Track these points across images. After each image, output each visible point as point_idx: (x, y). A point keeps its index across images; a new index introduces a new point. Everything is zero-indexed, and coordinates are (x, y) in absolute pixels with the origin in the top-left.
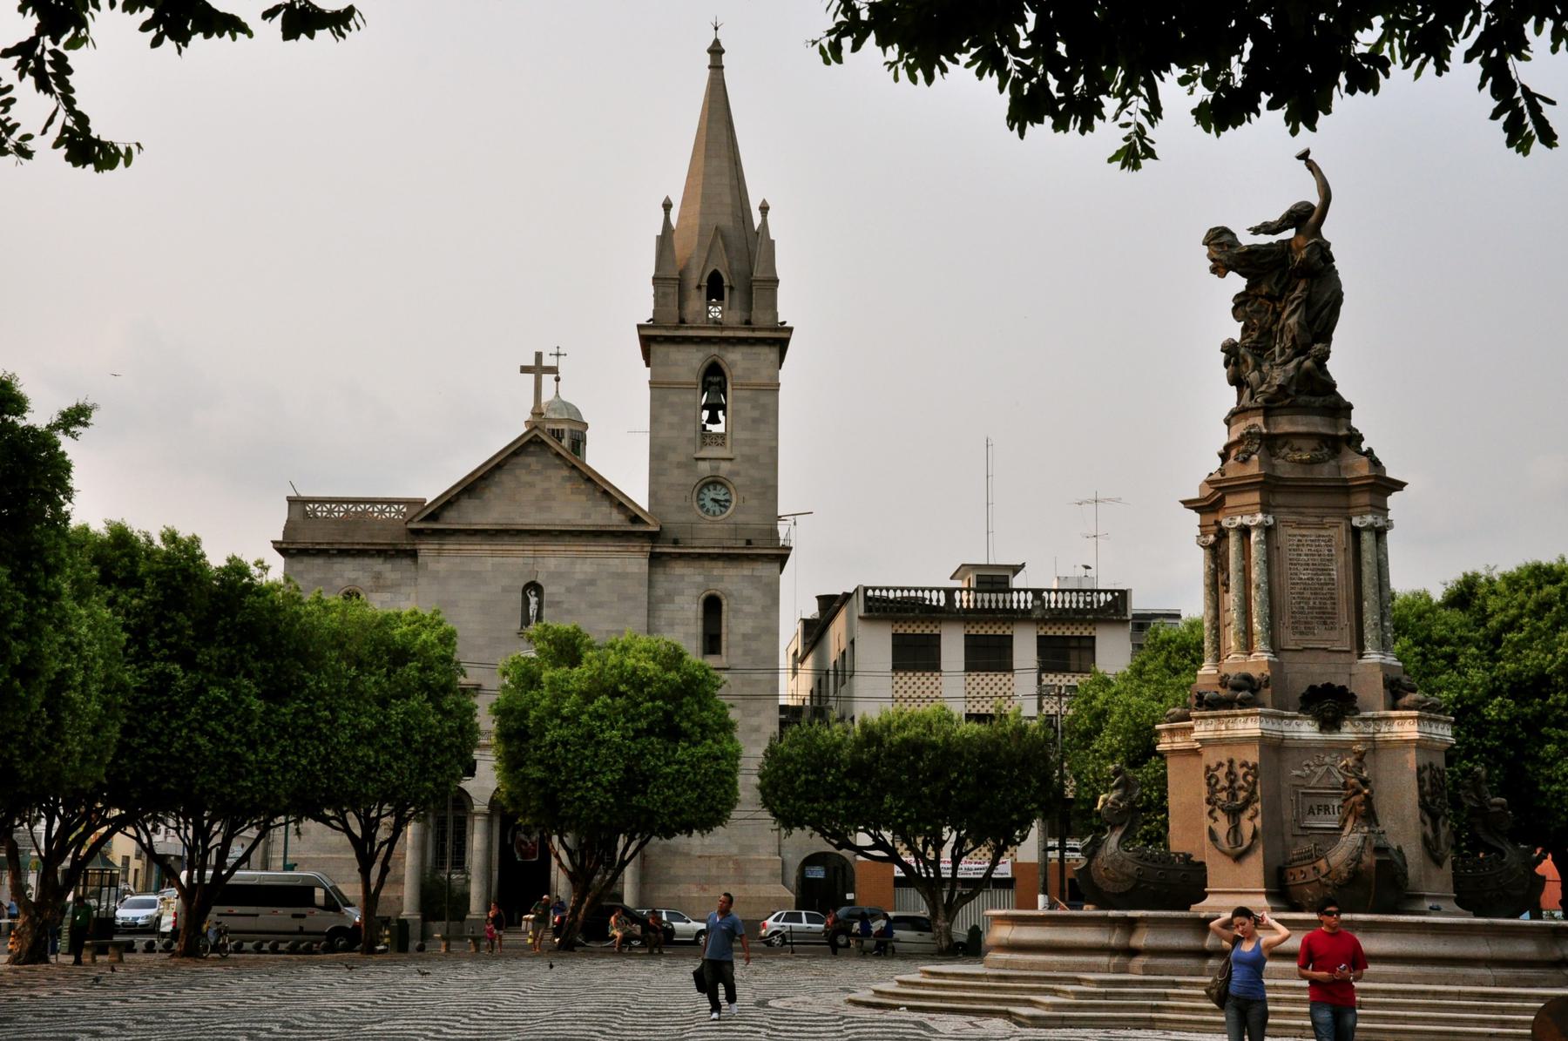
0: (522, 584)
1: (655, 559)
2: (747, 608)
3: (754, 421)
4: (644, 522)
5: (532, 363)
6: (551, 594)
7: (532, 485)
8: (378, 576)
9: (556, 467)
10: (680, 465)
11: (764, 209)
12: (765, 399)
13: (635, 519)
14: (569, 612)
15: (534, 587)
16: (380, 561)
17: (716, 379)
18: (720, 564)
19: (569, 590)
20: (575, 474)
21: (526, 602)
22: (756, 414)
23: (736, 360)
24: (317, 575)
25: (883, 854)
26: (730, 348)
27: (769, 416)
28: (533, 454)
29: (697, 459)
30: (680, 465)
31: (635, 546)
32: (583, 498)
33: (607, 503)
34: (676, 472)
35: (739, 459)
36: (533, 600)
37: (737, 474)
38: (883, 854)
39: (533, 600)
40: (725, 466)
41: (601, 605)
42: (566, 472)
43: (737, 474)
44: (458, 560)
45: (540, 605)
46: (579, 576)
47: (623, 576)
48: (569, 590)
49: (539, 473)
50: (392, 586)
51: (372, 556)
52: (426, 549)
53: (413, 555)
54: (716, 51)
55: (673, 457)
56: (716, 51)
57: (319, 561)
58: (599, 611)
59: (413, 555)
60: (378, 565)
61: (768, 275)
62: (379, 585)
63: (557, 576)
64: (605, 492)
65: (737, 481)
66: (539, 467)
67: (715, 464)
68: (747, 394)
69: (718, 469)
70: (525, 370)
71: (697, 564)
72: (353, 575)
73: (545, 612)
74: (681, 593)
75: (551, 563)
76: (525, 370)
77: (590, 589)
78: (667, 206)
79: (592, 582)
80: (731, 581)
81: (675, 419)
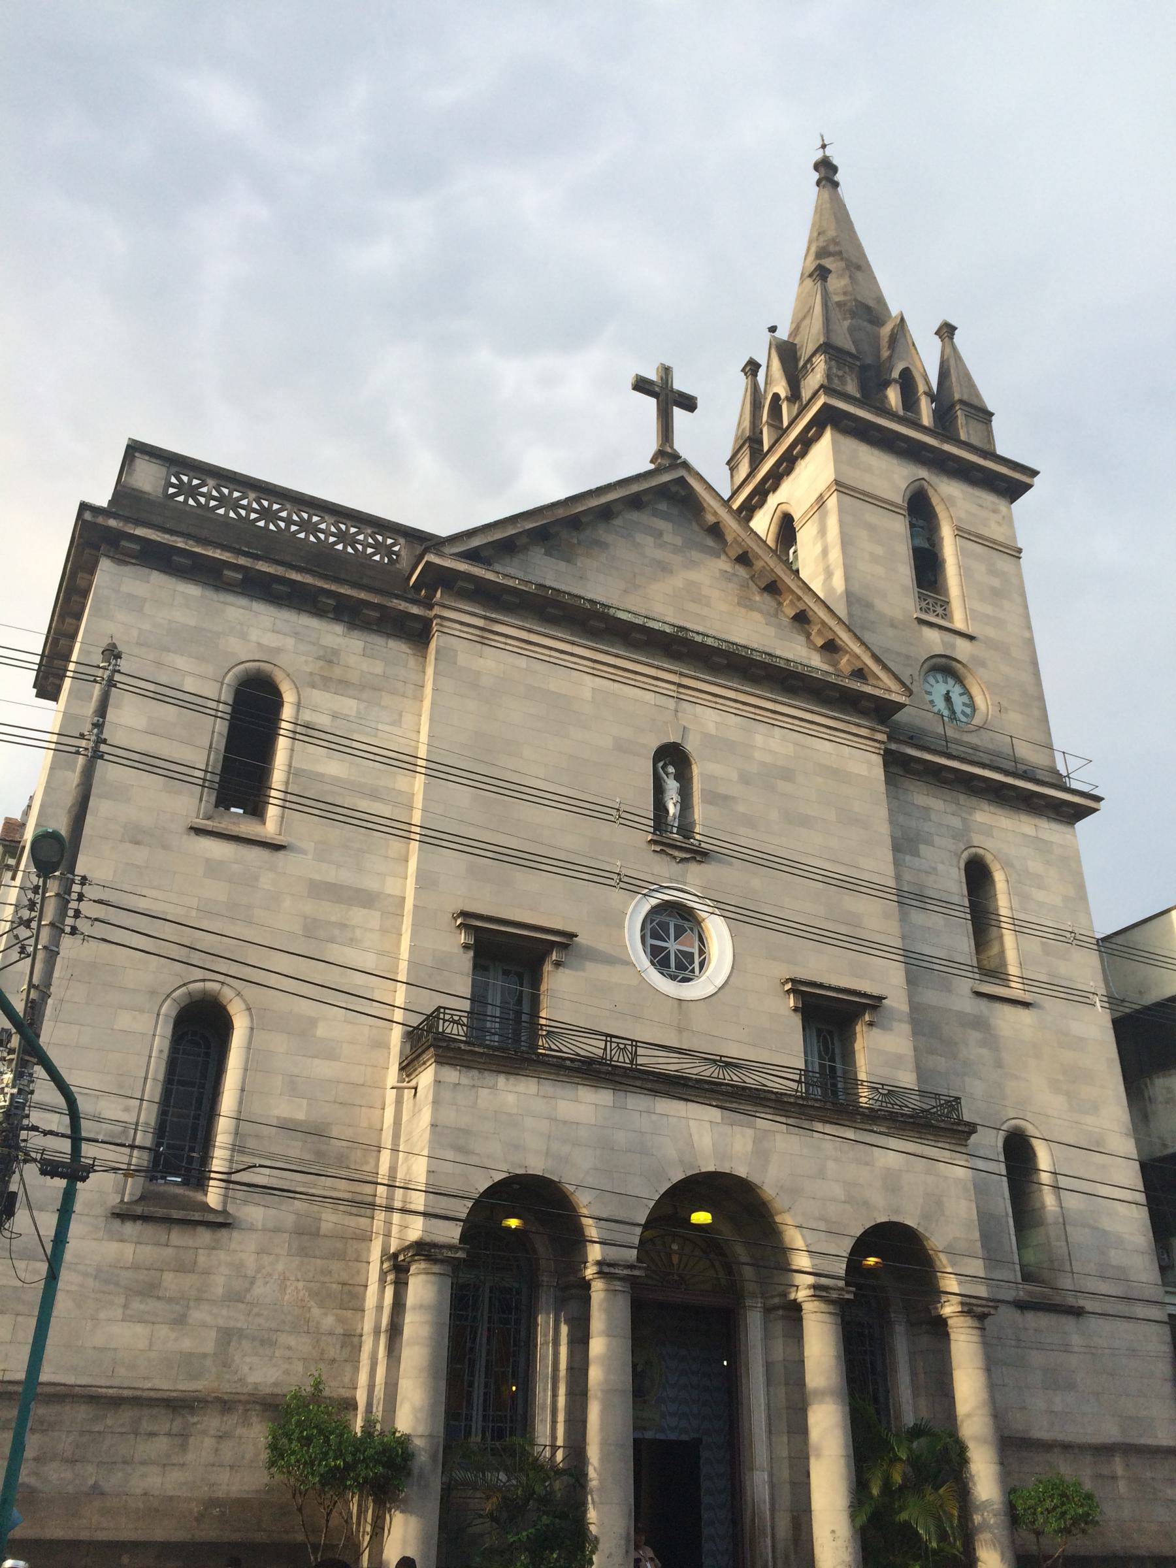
0: (654, 744)
7: (665, 569)
8: (330, 658)
11: (947, 331)
12: (1004, 564)
15: (672, 758)
16: (339, 628)
19: (745, 779)
22: (996, 582)
24: (184, 617)
26: (945, 479)
27: (1011, 592)
28: (666, 517)
29: (921, 621)
32: (756, 616)
36: (672, 786)
39: (672, 786)
40: (960, 643)
41: (805, 821)
44: (522, 662)
47: (838, 775)
48: (745, 779)
49: (677, 550)
50: (363, 687)
51: (319, 612)
54: (826, 170)
56: (826, 170)
57: (193, 591)
59: (417, 634)
62: (329, 677)
63: (719, 745)
66: (678, 541)
68: (979, 549)
70: (642, 385)
72: (271, 640)
77: (784, 786)
79: (787, 775)
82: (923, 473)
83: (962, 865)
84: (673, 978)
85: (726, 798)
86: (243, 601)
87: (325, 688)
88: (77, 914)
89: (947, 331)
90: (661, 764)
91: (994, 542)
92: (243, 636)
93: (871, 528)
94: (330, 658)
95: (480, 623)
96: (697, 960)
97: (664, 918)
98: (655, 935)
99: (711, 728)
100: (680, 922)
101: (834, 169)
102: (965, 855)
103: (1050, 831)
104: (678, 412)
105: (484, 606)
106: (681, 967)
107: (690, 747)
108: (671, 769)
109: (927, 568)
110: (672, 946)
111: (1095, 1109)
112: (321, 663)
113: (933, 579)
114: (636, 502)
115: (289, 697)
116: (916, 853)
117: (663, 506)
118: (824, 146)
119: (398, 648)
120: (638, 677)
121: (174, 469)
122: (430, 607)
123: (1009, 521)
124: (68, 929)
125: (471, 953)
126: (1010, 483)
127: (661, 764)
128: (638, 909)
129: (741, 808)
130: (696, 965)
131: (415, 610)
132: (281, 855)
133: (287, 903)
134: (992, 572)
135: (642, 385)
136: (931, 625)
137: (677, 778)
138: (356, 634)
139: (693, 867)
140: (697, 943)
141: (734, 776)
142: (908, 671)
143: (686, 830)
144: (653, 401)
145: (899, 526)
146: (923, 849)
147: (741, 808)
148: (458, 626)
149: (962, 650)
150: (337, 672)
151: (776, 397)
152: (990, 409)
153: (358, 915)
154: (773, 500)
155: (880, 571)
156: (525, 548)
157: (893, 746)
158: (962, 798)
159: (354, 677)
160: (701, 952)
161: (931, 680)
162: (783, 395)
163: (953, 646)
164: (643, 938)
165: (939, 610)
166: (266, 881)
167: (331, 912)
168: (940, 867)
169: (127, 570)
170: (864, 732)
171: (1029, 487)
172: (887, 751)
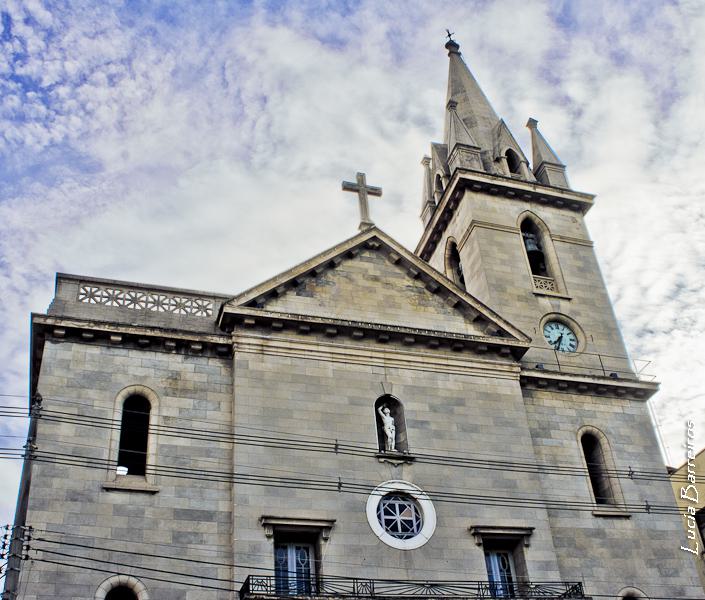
0: (376, 397)
1: (525, 382)
5: (354, 181)
11: (532, 123)
13: (501, 333)
15: (387, 402)
16: (179, 358)
21: (380, 423)
22: (580, 264)
23: (545, 214)
27: (589, 267)
30: (520, 298)
31: (504, 364)
34: (518, 304)
35: (575, 300)
36: (388, 421)
39: (388, 421)
40: (563, 303)
41: (475, 429)
42: (408, 282)
43: (578, 313)
45: (399, 427)
46: (442, 393)
47: (491, 397)
48: (434, 409)
52: (246, 342)
53: (226, 354)
56: (452, 47)
58: (475, 436)
60: (175, 362)
63: (414, 390)
67: (555, 301)
73: (411, 433)
75: (406, 374)
77: (458, 410)
79: (460, 402)
80: (604, 415)
82: (527, 206)
83: (579, 439)
84: (401, 537)
85: (423, 422)
86: (124, 352)
87: (174, 395)
88: (28, 548)
90: (381, 408)
91: (576, 240)
92: (125, 373)
93: (500, 245)
94: (175, 377)
96: (415, 524)
97: (391, 501)
98: (387, 513)
99: (410, 382)
100: (402, 502)
101: (457, 46)
102: (580, 433)
103: (629, 406)
104: (370, 198)
105: (262, 333)
106: (405, 529)
107: (395, 394)
108: (387, 410)
109: (538, 262)
110: (398, 518)
111: (676, 573)
112: (170, 381)
113: (542, 267)
114: (349, 255)
115: (154, 404)
116: (549, 437)
117: (367, 254)
118: (449, 35)
119: (214, 364)
120: (361, 359)
121: (82, 285)
122: (231, 337)
123: (582, 226)
124: (24, 557)
125: (272, 540)
126: (579, 206)
127: (381, 408)
128: (373, 501)
130: (415, 527)
131: (221, 341)
132: (156, 497)
133: (162, 525)
134: (577, 258)
135: (348, 187)
137: (391, 415)
138: (190, 360)
139: (406, 469)
140: (414, 513)
142: (532, 326)
144: (356, 194)
145: (518, 239)
147: (433, 427)
148: (247, 347)
150: (180, 385)
151: (439, 176)
153: (204, 526)
154: (445, 236)
156: (284, 293)
157: (526, 374)
159: (190, 386)
160: (417, 519)
161: (549, 329)
162: (442, 175)
163: (559, 306)
164: (379, 517)
165: (549, 286)
166: (148, 514)
167: (188, 526)
168: (565, 442)
169: (58, 346)
170: (506, 368)
171: (591, 205)
172: (522, 377)
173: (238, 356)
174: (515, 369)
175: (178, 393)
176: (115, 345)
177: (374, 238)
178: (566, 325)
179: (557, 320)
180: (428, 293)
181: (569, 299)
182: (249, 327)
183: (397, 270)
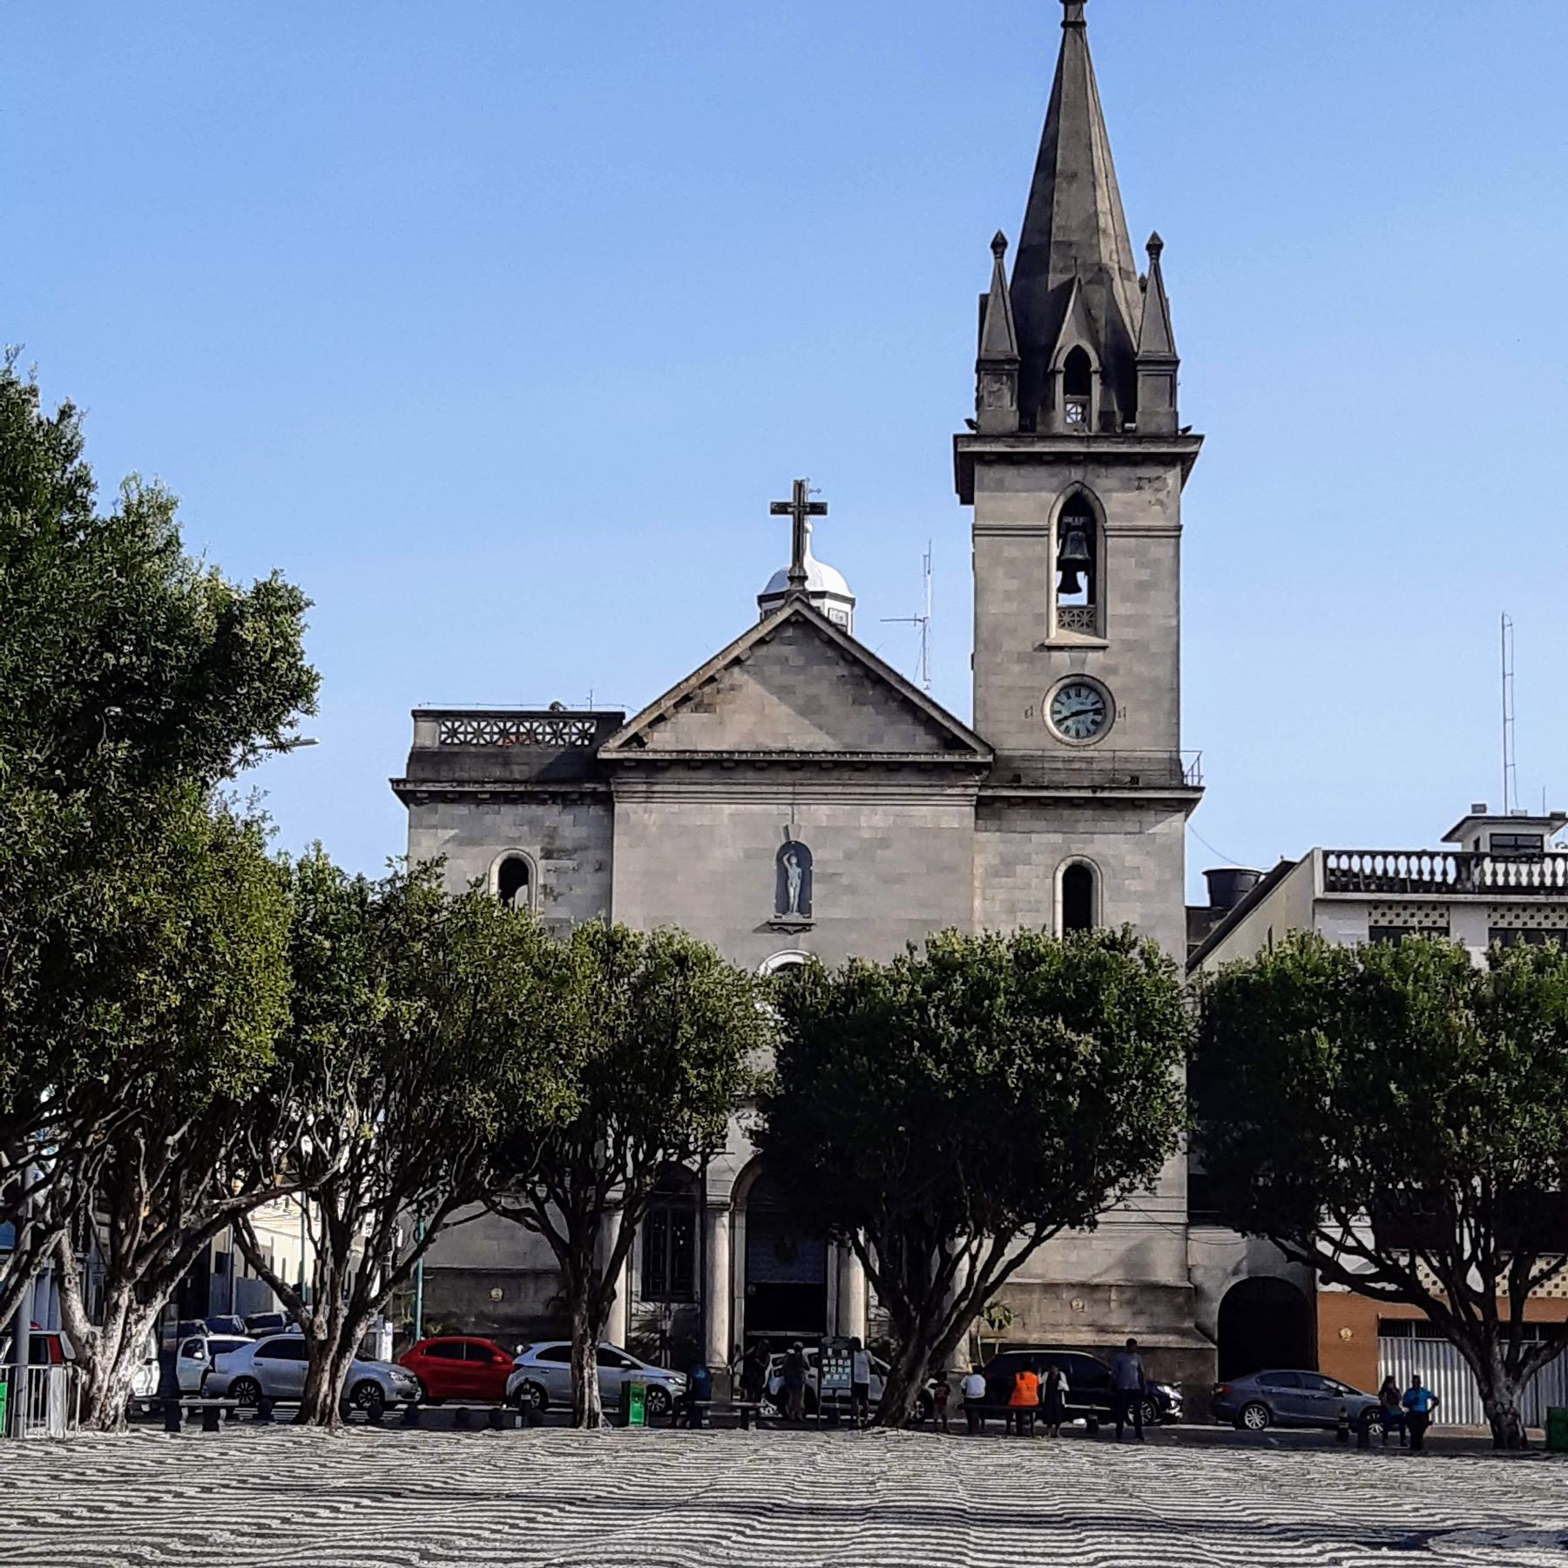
1: (984, 807)
2: (1133, 885)
3: (1142, 586)
4: (967, 747)
5: (788, 497)
6: (824, 862)
9: (828, 661)
10: (1021, 658)
11: (1155, 247)
12: (1159, 550)
13: (951, 742)
14: (850, 890)
15: (795, 852)
16: (556, 809)
17: (1079, 521)
18: (1088, 813)
20: (857, 670)
22: (1144, 575)
25: (1392, 1287)
30: (1021, 658)
33: (909, 718)
34: (1016, 668)
35: (1114, 647)
36: (794, 872)
37: (1113, 670)
38: (1392, 1287)
39: (794, 872)
41: (900, 879)
42: (842, 670)
43: (1113, 670)
47: (937, 832)
48: (849, 856)
49: (801, 670)
55: (1010, 645)
59: (607, 801)
61: (1164, 353)
63: (827, 833)
64: (906, 701)
65: (1112, 683)
66: (801, 661)
69: (1084, 662)
70: (780, 509)
71: (1051, 813)
73: (816, 889)
74: (1027, 862)
75: (819, 817)
76: (780, 509)
78: (999, 245)
79: (884, 843)
81: (1013, 585)
82: (1076, 474)
89: (1155, 247)
95: (644, 788)
129: (845, 881)
131: (601, 788)
136: (1060, 648)
137: (798, 865)
139: (802, 935)
141: (841, 855)
143: (805, 907)
146: (1019, 869)
147: (845, 881)
149: (1093, 664)
152: (1180, 356)
155: (1012, 607)
158: (1066, 813)
169: (423, 808)
173: (619, 808)
174: (971, 791)
175: (588, 801)
176: (484, 801)
177: (797, 612)
178: (1092, 689)
179: (1079, 685)
180: (867, 683)
181: (1104, 648)
182: (630, 768)
183: (830, 653)
